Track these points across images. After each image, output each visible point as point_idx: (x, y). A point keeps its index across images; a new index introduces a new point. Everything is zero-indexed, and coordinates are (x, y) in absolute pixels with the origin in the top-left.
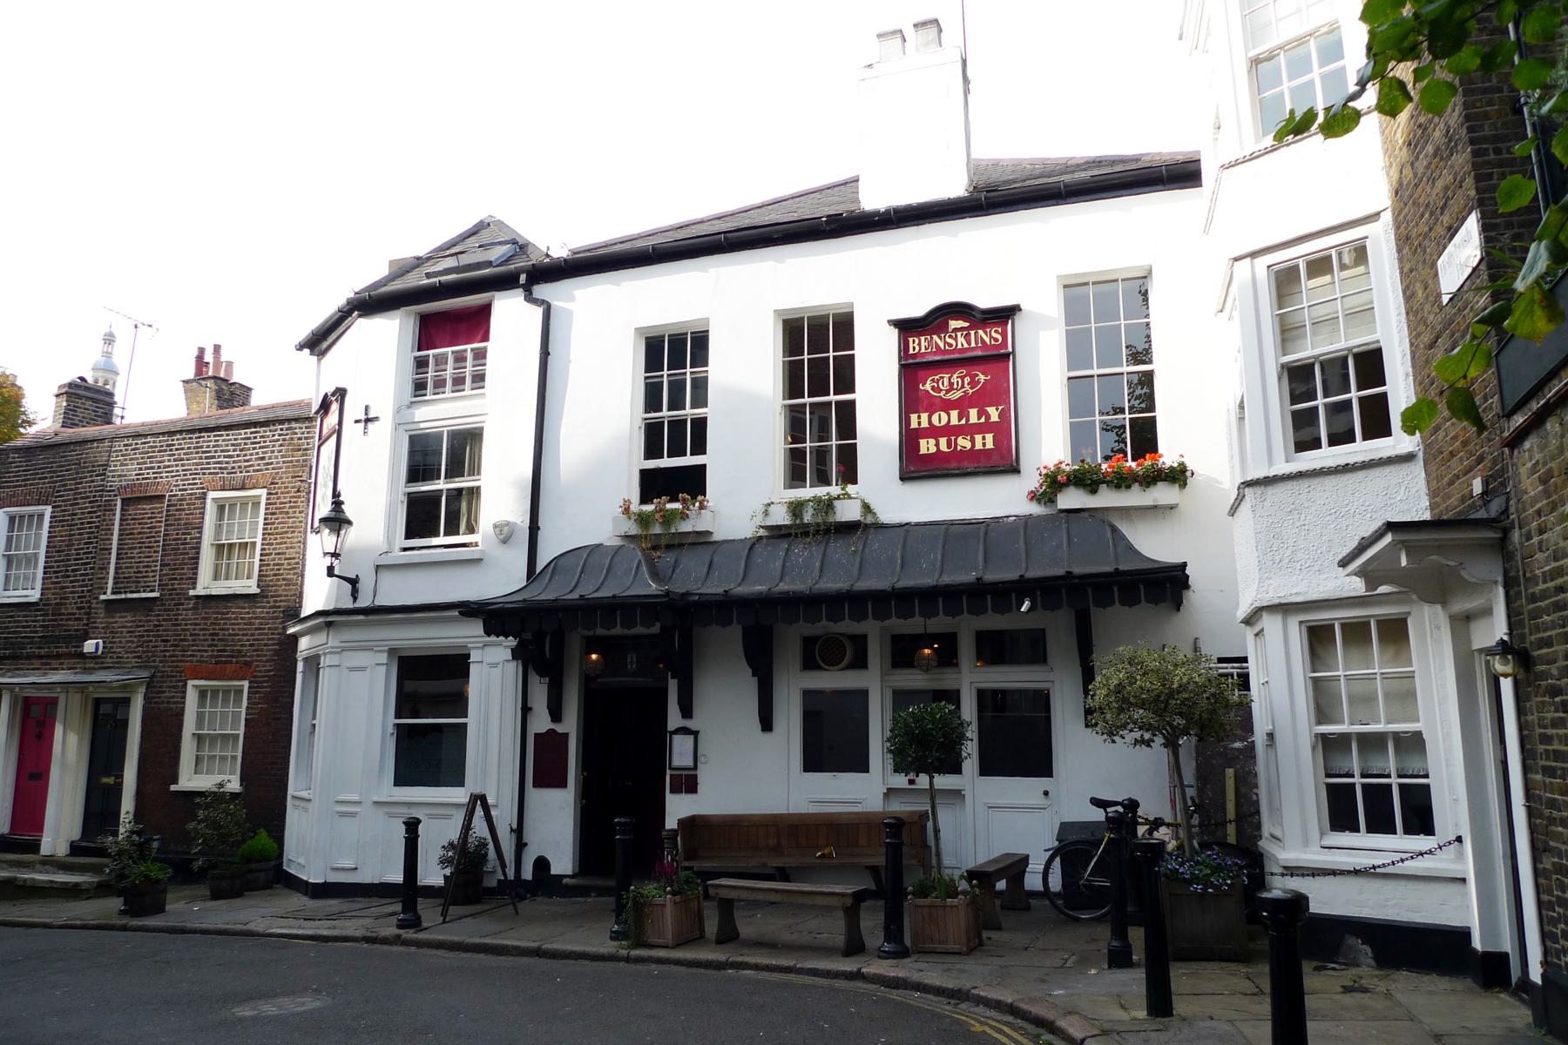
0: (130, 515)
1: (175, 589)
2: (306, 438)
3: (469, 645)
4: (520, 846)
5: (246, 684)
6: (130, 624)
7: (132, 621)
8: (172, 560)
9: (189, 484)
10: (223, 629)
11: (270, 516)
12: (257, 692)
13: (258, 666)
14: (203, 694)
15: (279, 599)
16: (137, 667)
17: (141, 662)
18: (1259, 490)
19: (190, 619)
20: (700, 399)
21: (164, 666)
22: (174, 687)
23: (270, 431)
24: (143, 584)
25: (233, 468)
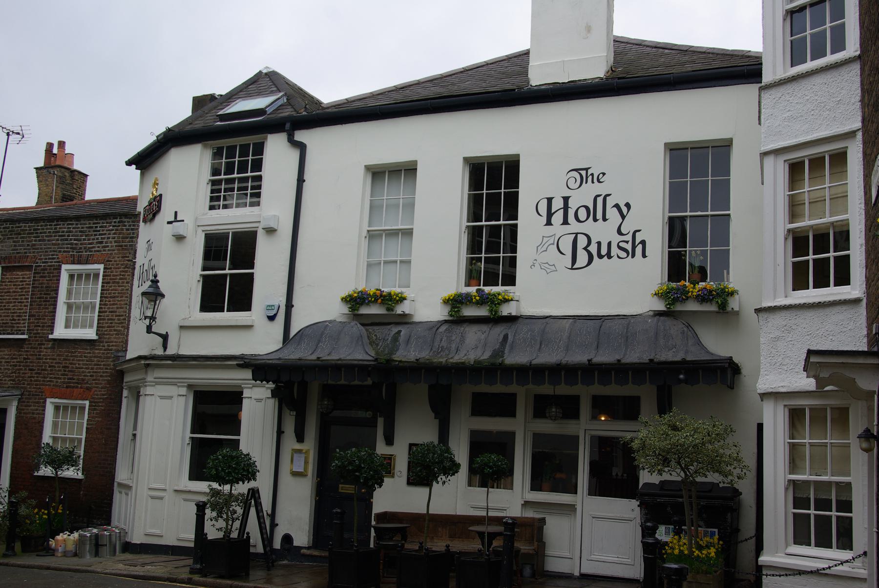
0: (7, 278)
1: (39, 334)
2: (132, 229)
3: (243, 386)
4: (274, 525)
5: (87, 403)
6: (7, 357)
7: (8, 355)
8: (36, 312)
9: (49, 259)
10: (71, 364)
11: (106, 285)
12: (95, 409)
13: (96, 391)
14: (57, 408)
15: (111, 344)
16: (11, 387)
17: (15, 384)
19: (49, 355)
21: (30, 388)
22: (38, 403)
23: (107, 223)
24: (16, 329)
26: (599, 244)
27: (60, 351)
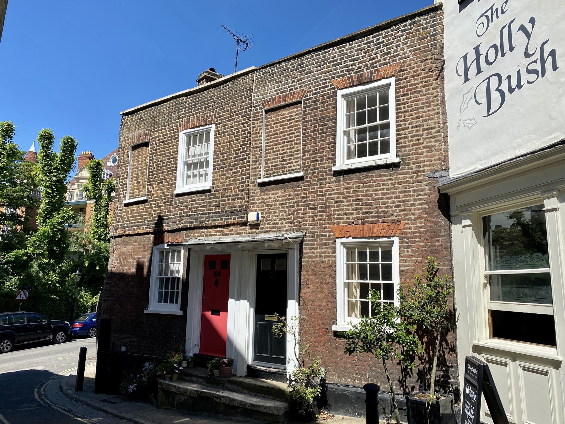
0: (273, 121)
1: (317, 169)
6: (281, 199)
7: (283, 196)
8: (312, 147)
11: (402, 98)
15: (422, 164)
16: (290, 230)
19: (333, 190)
21: (313, 228)
22: (325, 244)
24: (288, 169)
25: (360, 67)
27: (348, 184)
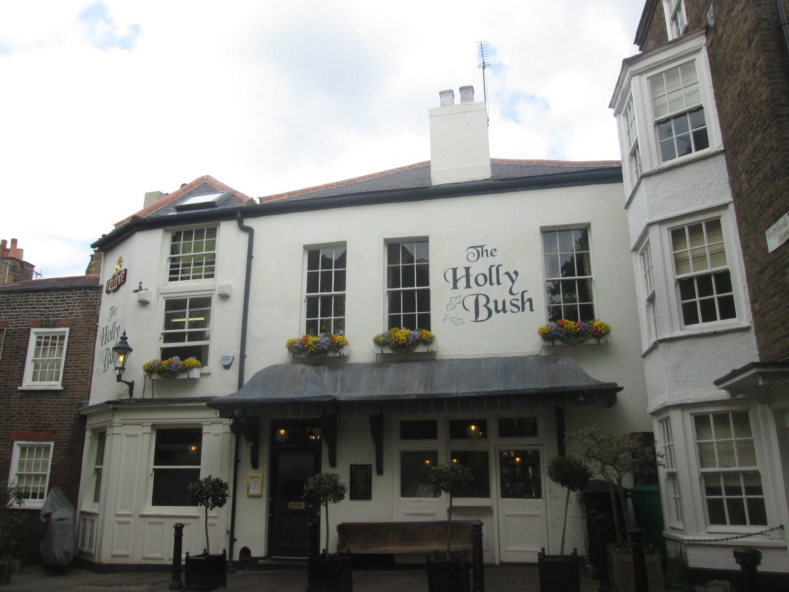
1: (8, 386)
2: (95, 299)
3: (202, 423)
4: (232, 540)
5: (52, 444)
9: (20, 323)
11: (71, 344)
12: (59, 449)
14: (23, 449)
15: (75, 393)
18: (667, 345)
19: (17, 404)
20: (341, 283)
22: (5, 445)
23: (73, 294)
25: (48, 315)
26: (496, 302)
27: (29, 401)
